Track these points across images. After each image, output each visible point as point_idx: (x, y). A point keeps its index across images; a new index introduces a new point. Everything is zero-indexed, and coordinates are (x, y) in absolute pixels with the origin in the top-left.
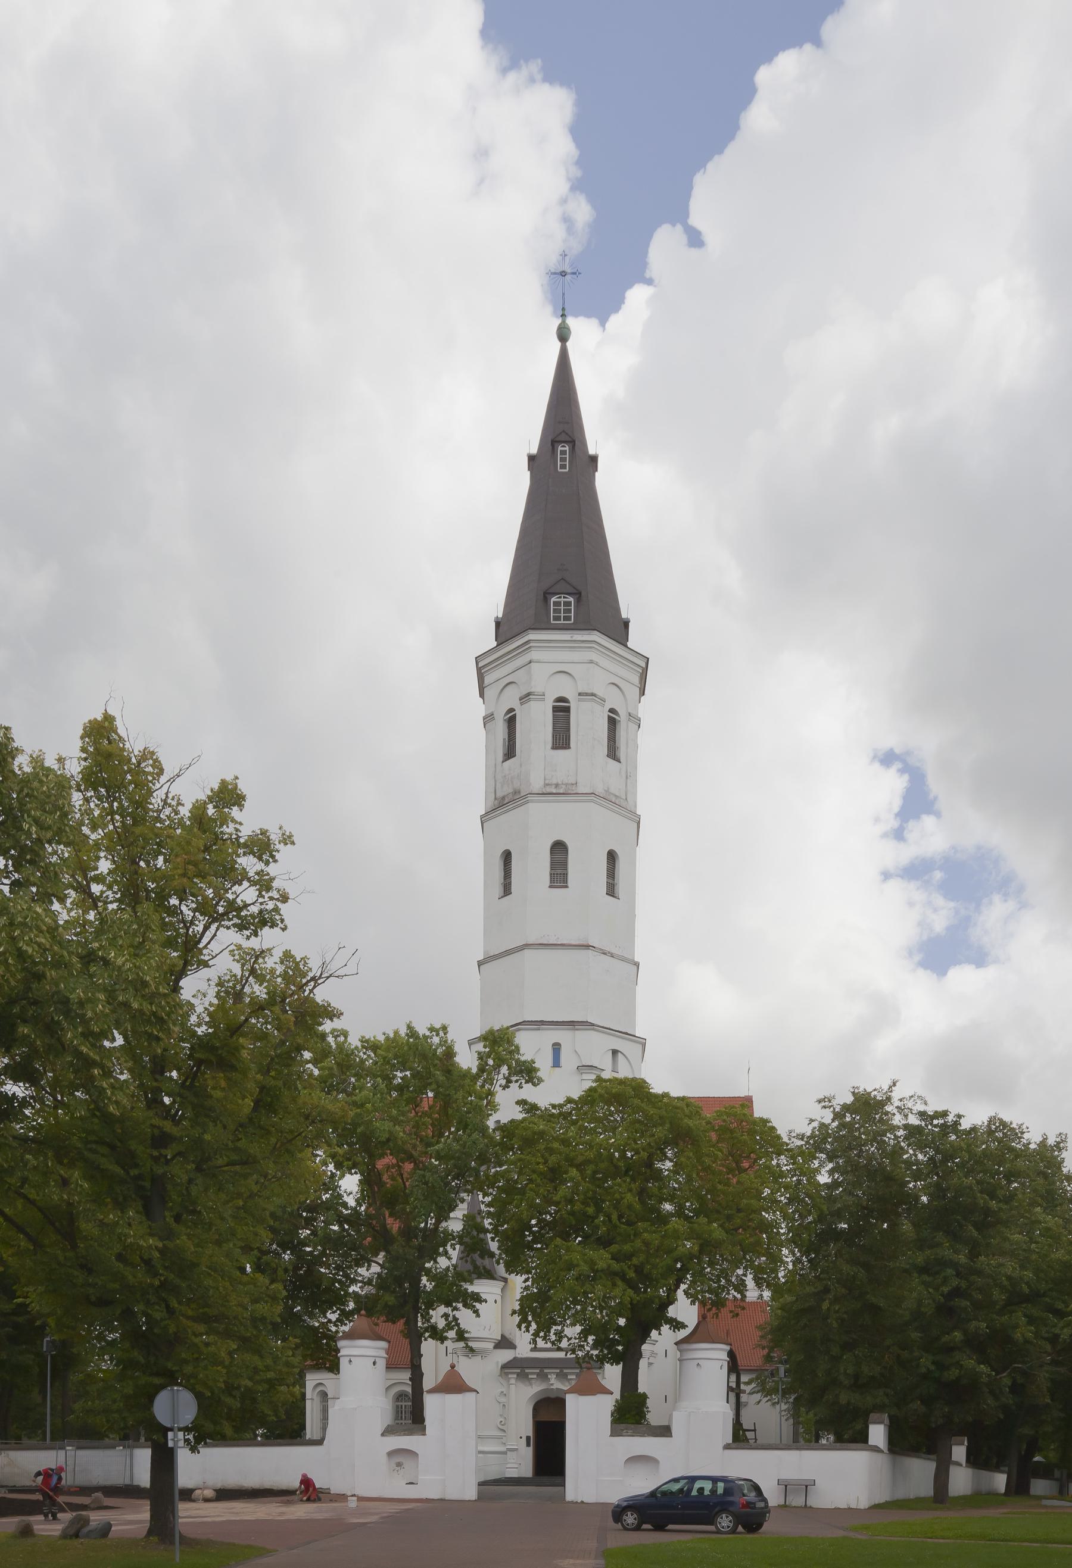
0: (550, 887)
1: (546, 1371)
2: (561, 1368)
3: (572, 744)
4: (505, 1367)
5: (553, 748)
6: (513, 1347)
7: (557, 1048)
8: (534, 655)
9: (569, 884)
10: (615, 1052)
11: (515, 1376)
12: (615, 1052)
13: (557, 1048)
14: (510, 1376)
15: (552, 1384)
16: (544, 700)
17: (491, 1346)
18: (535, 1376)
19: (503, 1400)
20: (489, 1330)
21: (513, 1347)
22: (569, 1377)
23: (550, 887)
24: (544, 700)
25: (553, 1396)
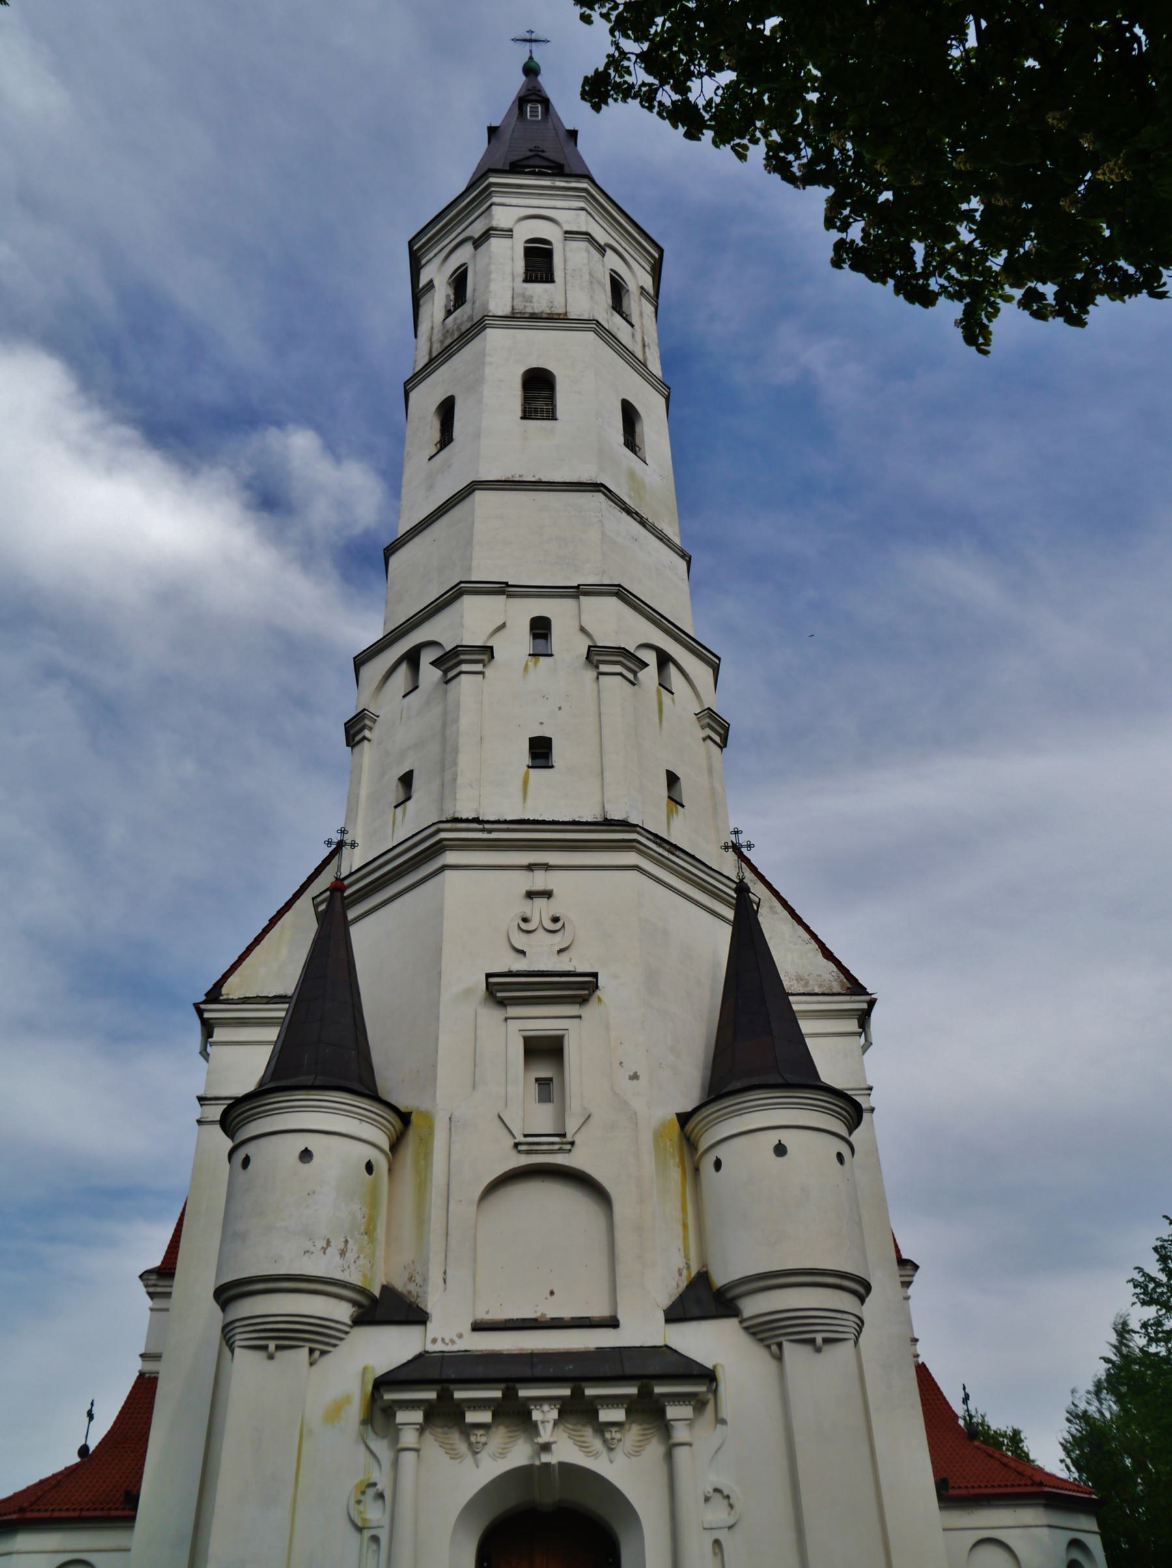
0: (522, 418)
1: (523, 1393)
2: (577, 1381)
3: (556, 278)
4: (383, 1383)
5: (526, 281)
6: (415, 1316)
7: (541, 628)
8: (495, 200)
9: (559, 414)
10: (664, 659)
11: (418, 1416)
12: (664, 659)
13: (541, 628)
14: (402, 1417)
15: (546, 1447)
16: (511, 237)
17: (342, 1312)
18: (485, 1417)
19: (374, 1514)
20: (343, 1253)
21: (415, 1316)
22: (605, 1415)
23: (522, 418)
24: (511, 237)
25: (547, 1498)
